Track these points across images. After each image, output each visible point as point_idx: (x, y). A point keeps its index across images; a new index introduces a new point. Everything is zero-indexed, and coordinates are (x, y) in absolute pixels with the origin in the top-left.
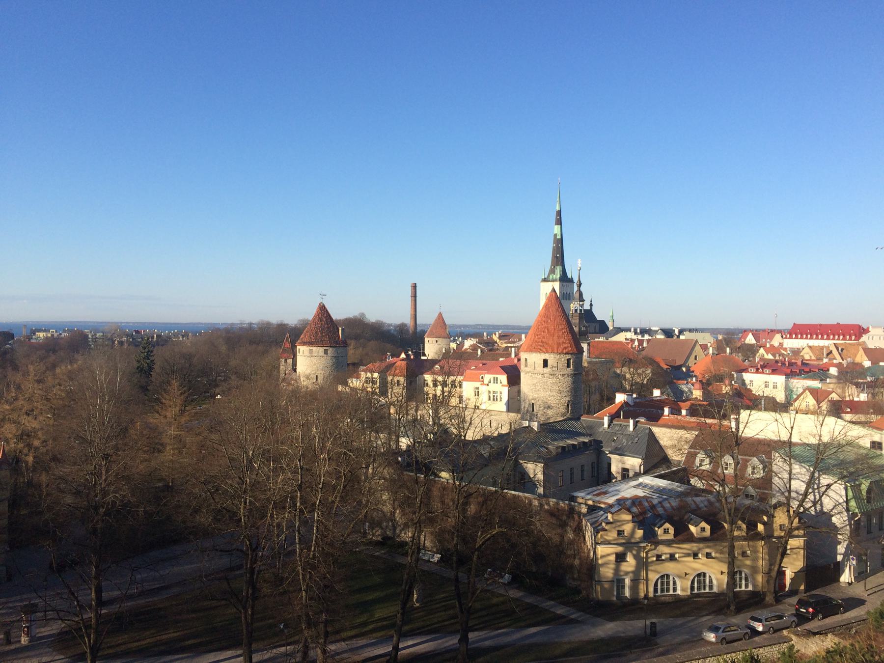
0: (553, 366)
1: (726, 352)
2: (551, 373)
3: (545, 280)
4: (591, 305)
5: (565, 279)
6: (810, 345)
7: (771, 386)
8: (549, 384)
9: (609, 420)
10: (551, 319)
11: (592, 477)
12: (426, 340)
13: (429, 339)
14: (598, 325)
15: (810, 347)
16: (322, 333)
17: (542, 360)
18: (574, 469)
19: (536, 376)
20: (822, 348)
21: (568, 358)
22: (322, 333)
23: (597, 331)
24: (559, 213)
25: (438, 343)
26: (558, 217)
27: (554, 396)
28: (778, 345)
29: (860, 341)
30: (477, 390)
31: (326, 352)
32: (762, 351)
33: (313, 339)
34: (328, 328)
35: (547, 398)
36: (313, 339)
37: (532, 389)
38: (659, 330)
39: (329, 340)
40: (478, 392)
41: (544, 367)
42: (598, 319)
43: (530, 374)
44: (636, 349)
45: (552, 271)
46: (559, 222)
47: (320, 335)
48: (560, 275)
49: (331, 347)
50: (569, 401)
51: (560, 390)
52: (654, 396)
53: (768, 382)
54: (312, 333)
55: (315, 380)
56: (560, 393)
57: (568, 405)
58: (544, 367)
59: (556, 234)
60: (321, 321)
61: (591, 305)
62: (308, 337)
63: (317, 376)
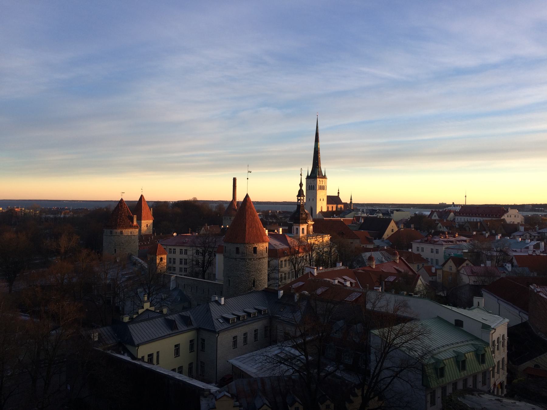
1: (410, 227)
4: (338, 193)
6: (469, 221)
7: (435, 251)
11: (265, 338)
12: (224, 218)
13: (225, 217)
15: (470, 223)
16: (121, 219)
18: (248, 333)
20: (477, 222)
21: (254, 246)
26: (317, 137)
28: (452, 219)
29: (502, 218)
32: (440, 225)
38: (377, 210)
39: (124, 225)
43: (227, 258)
46: (317, 140)
53: (433, 249)
55: (114, 253)
61: (338, 193)
63: (115, 250)
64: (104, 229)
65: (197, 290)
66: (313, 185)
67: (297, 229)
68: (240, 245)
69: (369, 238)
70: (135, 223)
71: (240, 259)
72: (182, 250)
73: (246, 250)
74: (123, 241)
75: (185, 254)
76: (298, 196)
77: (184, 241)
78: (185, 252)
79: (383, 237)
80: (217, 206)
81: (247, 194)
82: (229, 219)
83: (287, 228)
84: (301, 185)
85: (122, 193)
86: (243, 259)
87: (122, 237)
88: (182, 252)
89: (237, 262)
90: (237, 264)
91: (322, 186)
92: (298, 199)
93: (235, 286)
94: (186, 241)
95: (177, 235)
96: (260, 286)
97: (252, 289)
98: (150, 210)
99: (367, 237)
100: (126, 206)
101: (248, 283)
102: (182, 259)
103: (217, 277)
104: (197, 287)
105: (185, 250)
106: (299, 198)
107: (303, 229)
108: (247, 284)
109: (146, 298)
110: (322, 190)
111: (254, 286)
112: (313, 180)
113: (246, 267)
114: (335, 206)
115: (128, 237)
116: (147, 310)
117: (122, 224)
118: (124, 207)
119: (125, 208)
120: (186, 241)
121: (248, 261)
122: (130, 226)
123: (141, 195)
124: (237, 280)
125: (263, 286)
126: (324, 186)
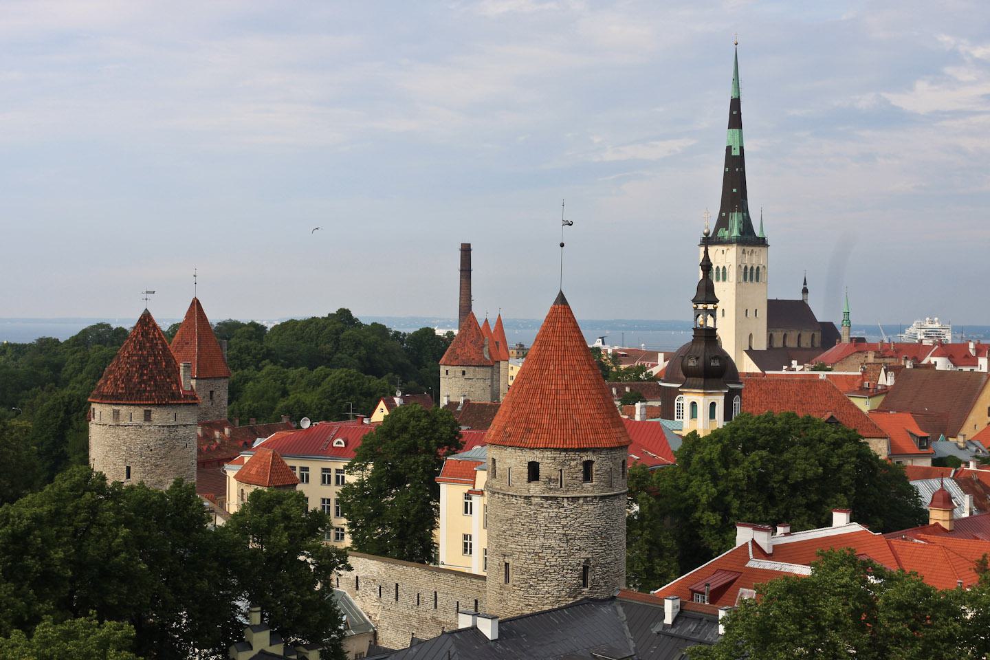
0: (550, 480)
2: (547, 495)
3: (708, 241)
4: (805, 291)
5: (749, 239)
8: (541, 521)
9: (673, 608)
10: (551, 368)
12: (443, 369)
13: (448, 368)
14: (818, 335)
16: (142, 375)
17: (527, 465)
19: (514, 501)
21: (585, 459)
22: (142, 375)
23: (817, 344)
24: (736, 104)
25: (466, 376)
26: (734, 113)
27: (553, 548)
30: (469, 501)
31: (147, 417)
33: (122, 388)
34: (155, 363)
35: (537, 554)
36: (122, 388)
37: (504, 532)
39: (155, 391)
40: (471, 503)
41: (529, 482)
42: (819, 321)
43: (501, 496)
44: (871, 391)
45: (722, 223)
46: (735, 121)
47: (135, 380)
48: (740, 229)
49: (158, 405)
50: (588, 560)
51: (564, 534)
52: (834, 524)
54: (121, 375)
55: (125, 475)
56: (568, 541)
57: (586, 569)
58: (529, 482)
59: (731, 146)
60: (140, 349)
61: (805, 291)
62: (111, 383)
63: (128, 469)
64: (93, 406)
65: (397, 595)
66: (724, 267)
67: (694, 404)
68: (542, 455)
69: (922, 439)
70: (188, 382)
71: (543, 497)
72: (328, 470)
73: (561, 470)
74: (152, 443)
75: (337, 483)
76: (696, 301)
77: (335, 445)
78: (338, 477)
79: (962, 432)
80: (416, 333)
81: (561, 292)
82: (461, 374)
83: (657, 404)
84: (707, 266)
85: (147, 292)
86: (551, 498)
87: (148, 429)
88: (329, 476)
89: (532, 507)
90: (532, 512)
91: (752, 268)
92: (695, 309)
93: (526, 583)
94: (339, 443)
95: (311, 424)
96: (606, 583)
97: (580, 593)
98: (222, 349)
99: (911, 433)
100: (159, 335)
101: (567, 573)
102: (329, 501)
103: (442, 558)
104: (397, 585)
105: (338, 471)
106: (701, 306)
107: (713, 405)
108: (563, 576)
109: (256, 618)
110: (751, 280)
111: (585, 585)
112: (724, 248)
113: (560, 523)
114: (793, 335)
115: (165, 428)
116: (262, 652)
117: (148, 389)
118: (154, 335)
119: (156, 338)
120: (339, 443)
121: (565, 505)
122: (173, 394)
123: (193, 302)
124: (534, 566)
125: (614, 585)
126: (758, 268)
